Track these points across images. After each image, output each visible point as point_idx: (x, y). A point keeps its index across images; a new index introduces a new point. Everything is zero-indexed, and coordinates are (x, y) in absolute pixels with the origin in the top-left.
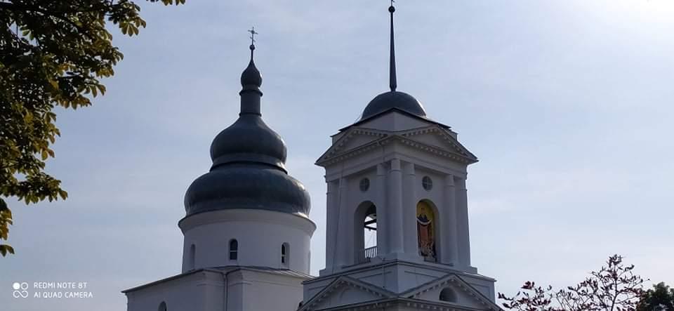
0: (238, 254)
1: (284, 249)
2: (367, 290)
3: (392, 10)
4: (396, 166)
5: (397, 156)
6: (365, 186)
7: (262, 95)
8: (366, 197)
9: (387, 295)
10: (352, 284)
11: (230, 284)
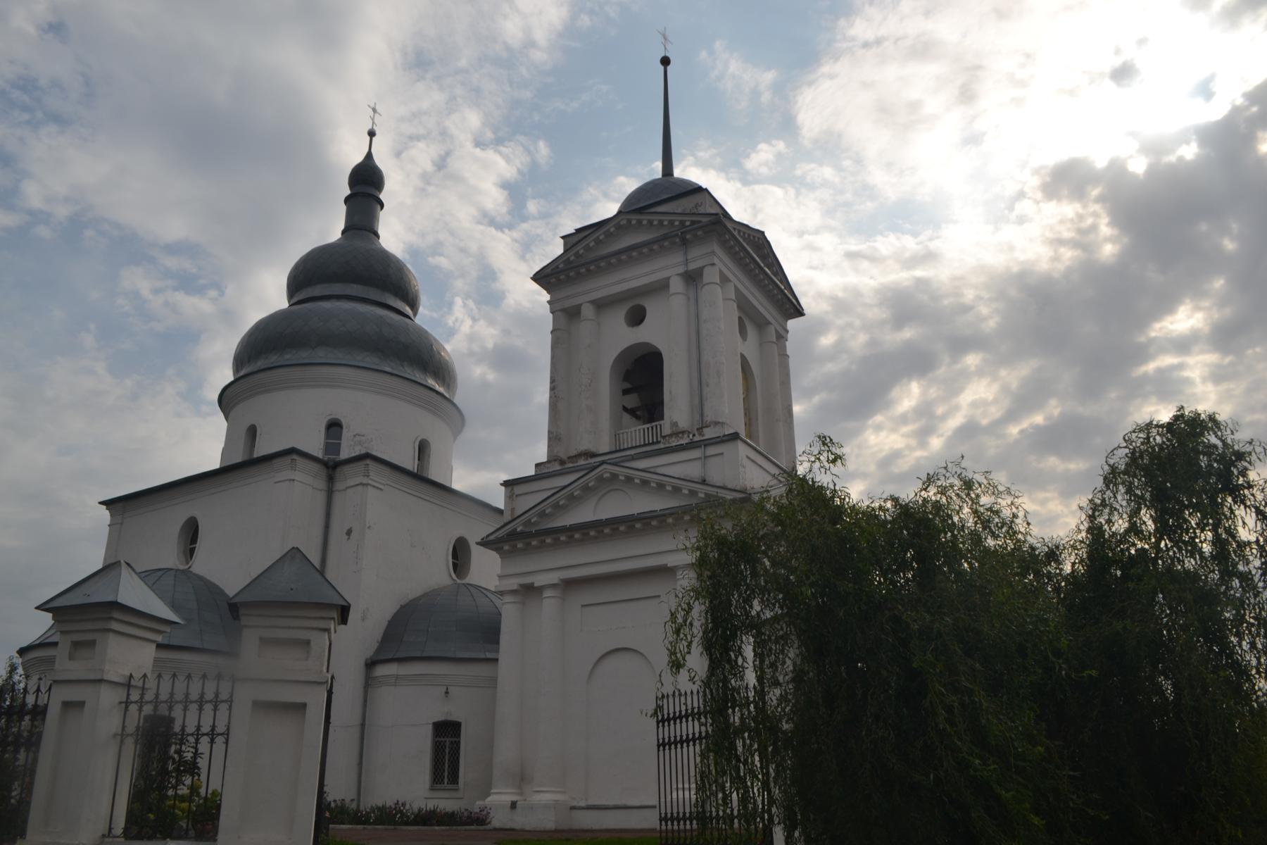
0: (342, 445)
1: (423, 449)
2: (669, 488)
3: (665, 61)
4: (711, 275)
5: (716, 261)
6: (637, 317)
7: (382, 206)
8: (644, 334)
9: (722, 493)
10: (629, 479)
11: (339, 486)
